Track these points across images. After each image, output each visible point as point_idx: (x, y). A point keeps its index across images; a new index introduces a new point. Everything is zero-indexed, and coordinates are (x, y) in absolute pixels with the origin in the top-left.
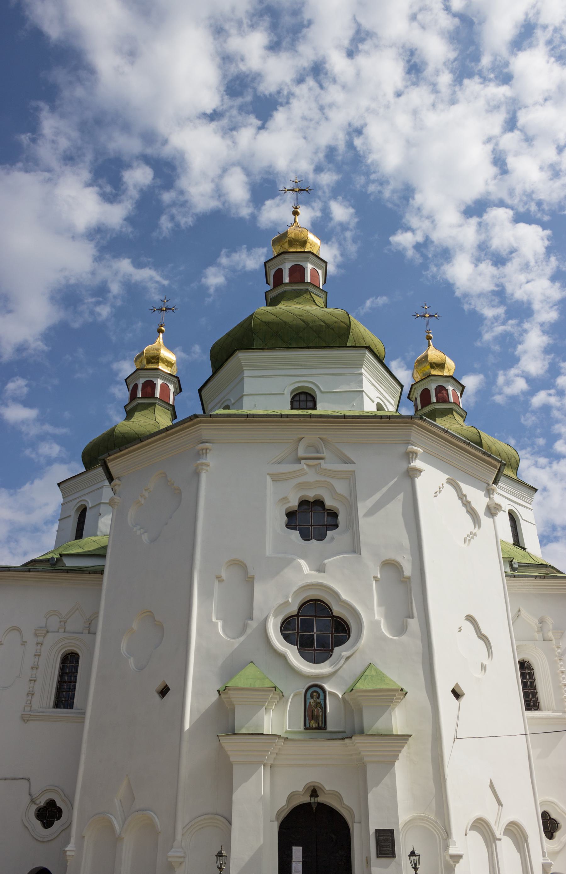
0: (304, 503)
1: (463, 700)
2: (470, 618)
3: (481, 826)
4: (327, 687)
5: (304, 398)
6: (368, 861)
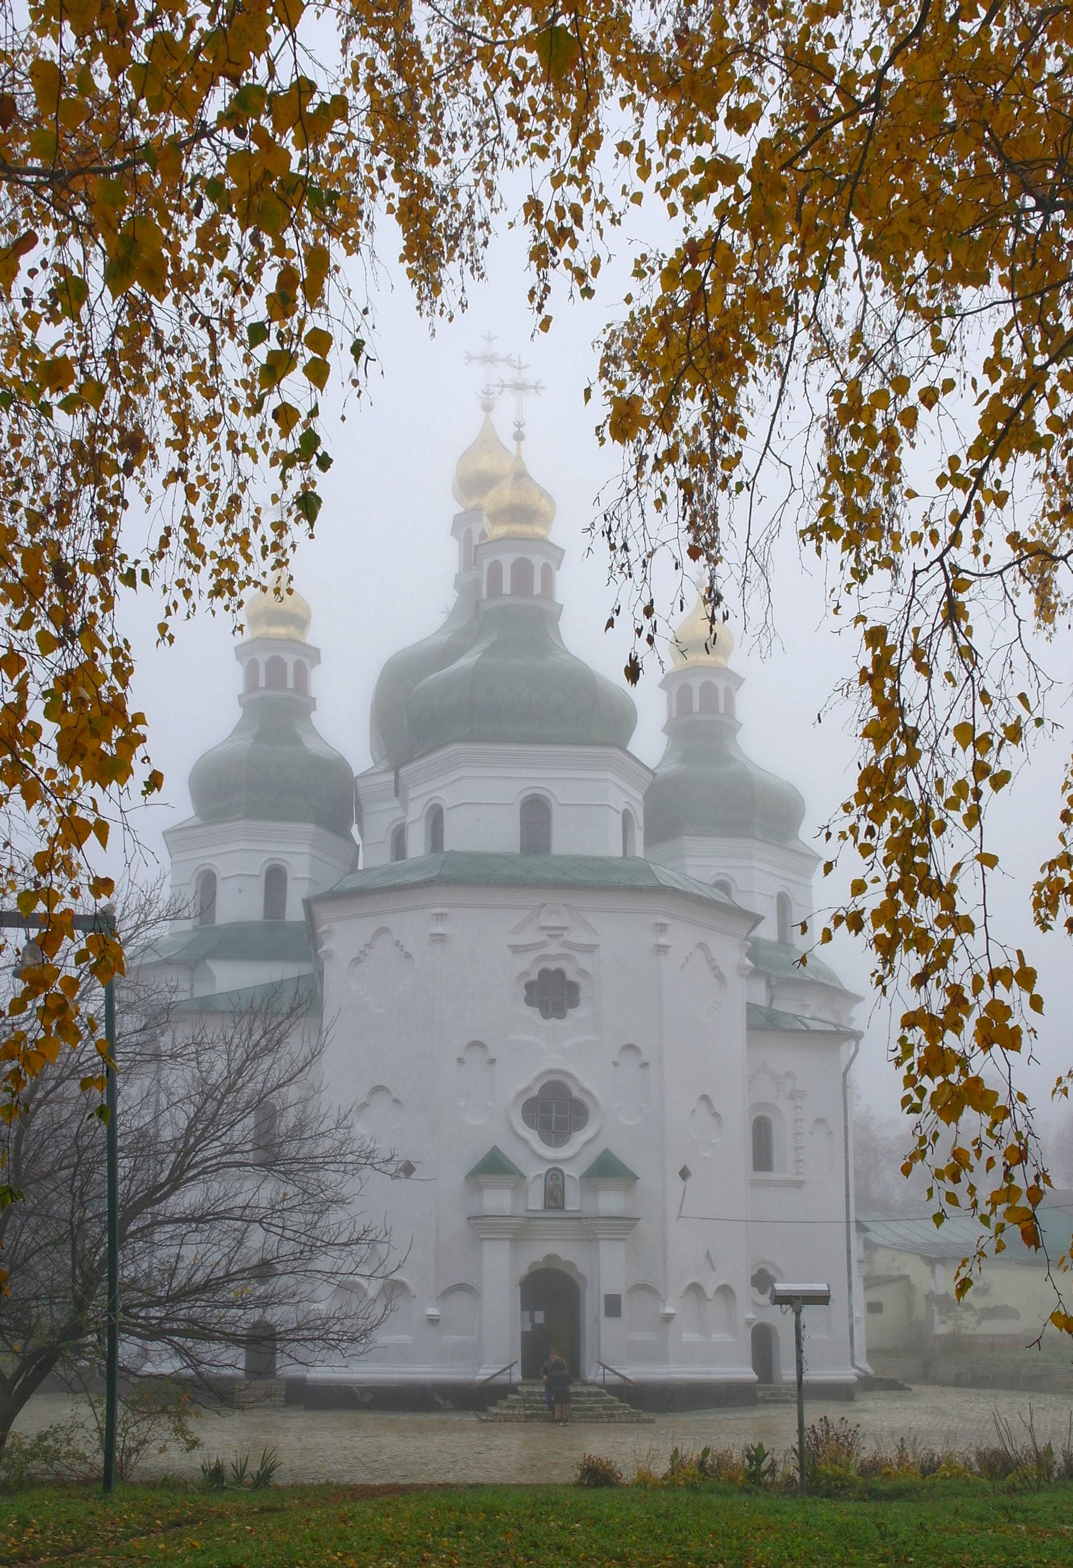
0: (544, 973)
1: (690, 1180)
2: (705, 1098)
4: (566, 1172)
6: (597, 1320)
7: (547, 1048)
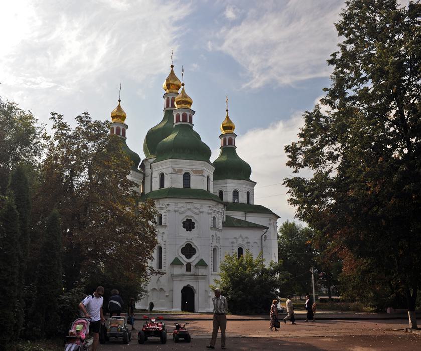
5: (187, 177)
7: (185, 236)
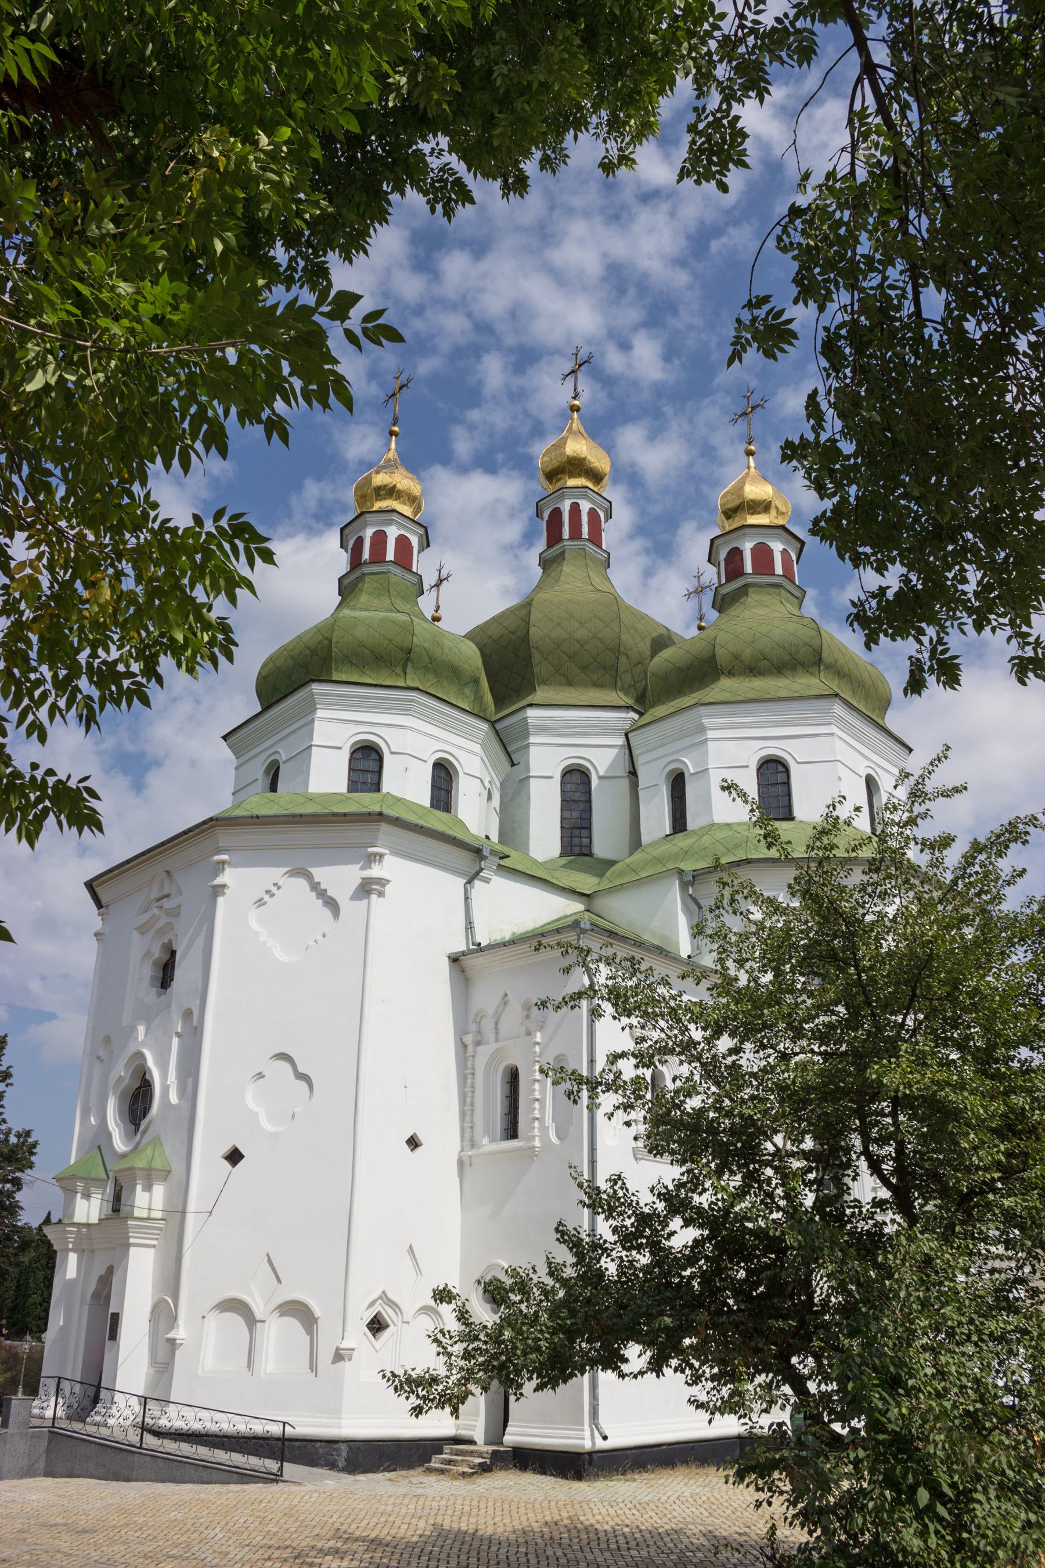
2: (284, 1057)
3: (237, 1306)
